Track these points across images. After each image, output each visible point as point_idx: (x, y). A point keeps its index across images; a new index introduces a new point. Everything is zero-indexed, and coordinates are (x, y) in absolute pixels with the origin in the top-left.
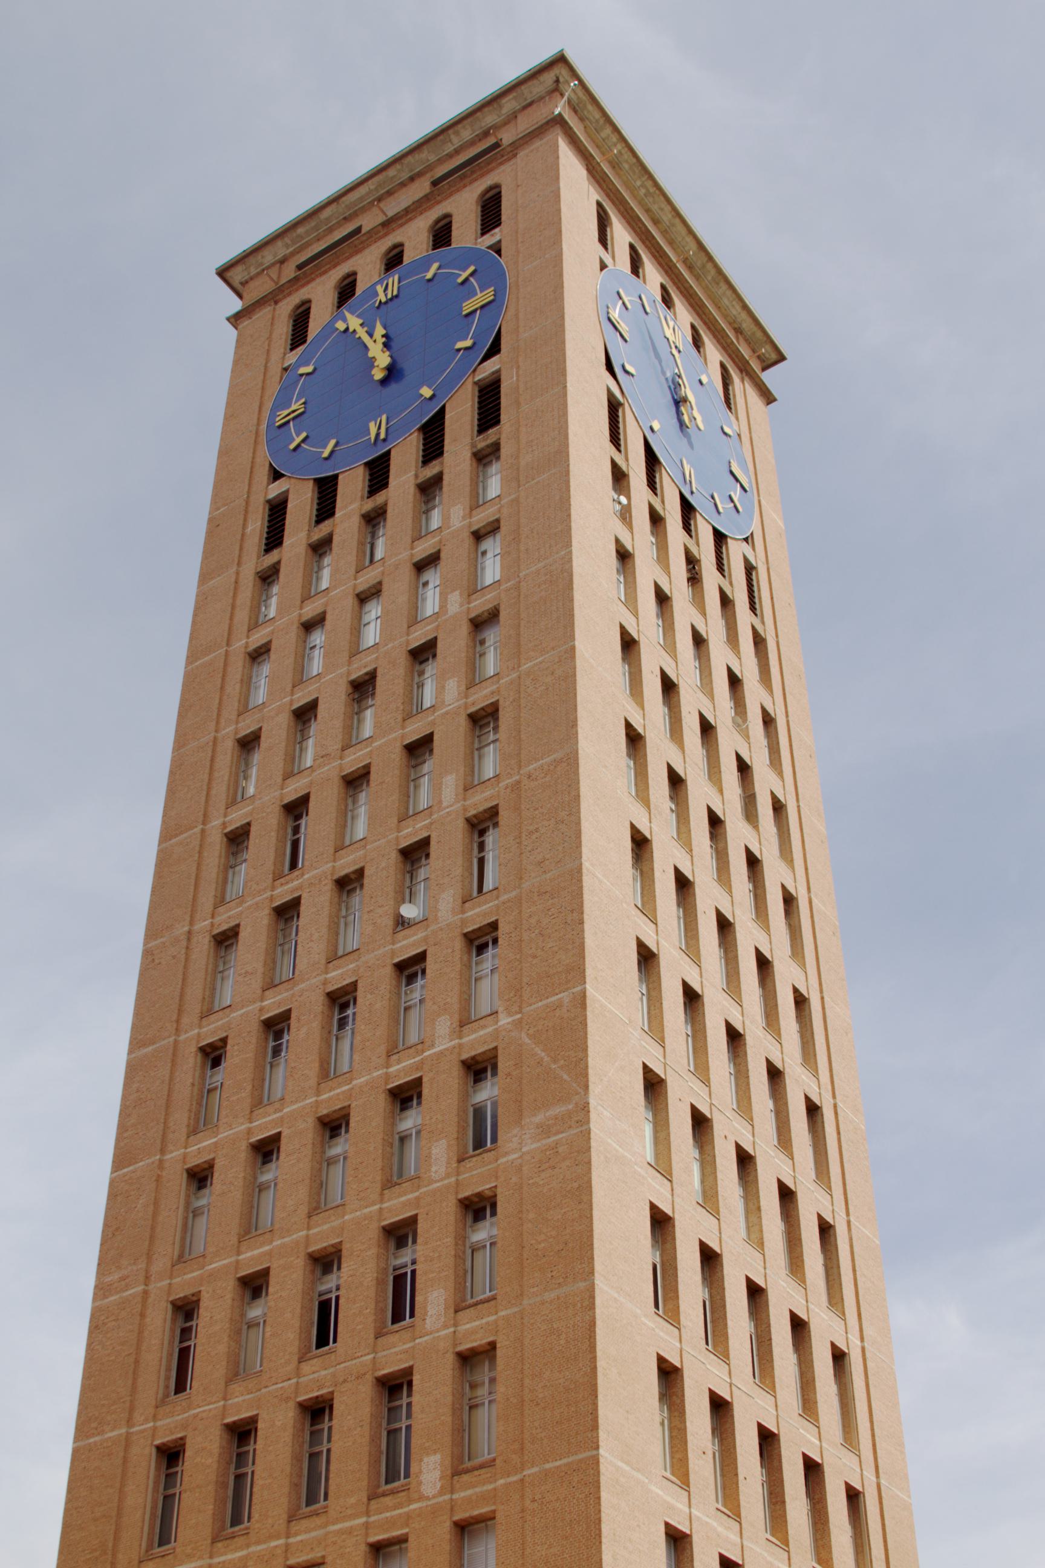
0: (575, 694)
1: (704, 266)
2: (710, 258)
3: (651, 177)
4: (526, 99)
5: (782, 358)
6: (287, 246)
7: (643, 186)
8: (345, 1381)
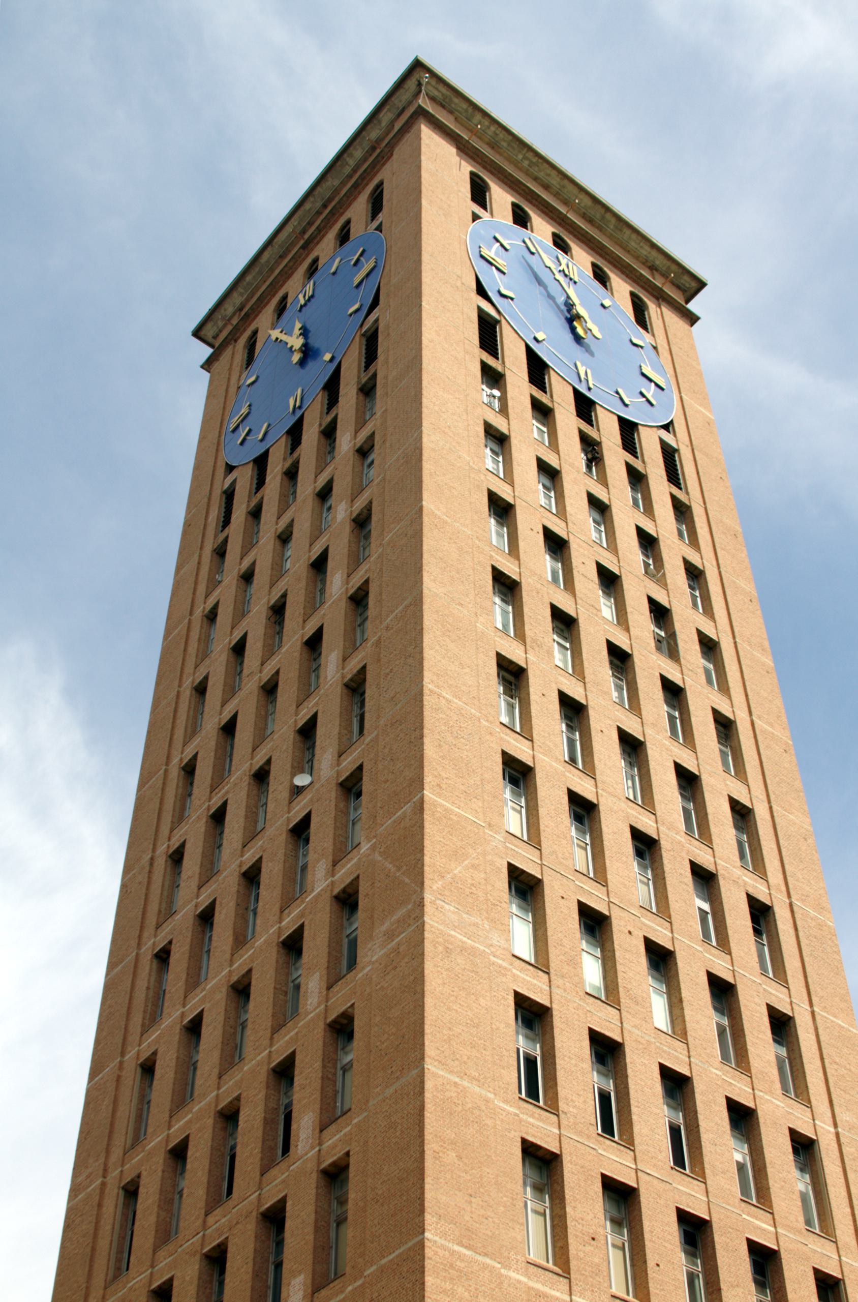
0: (422, 545)
1: (603, 217)
2: (607, 209)
3: (530, 149)
4: (398, 108)
5: (702, 285)
6: (242, 295)
7: (525, 158)
8: (237, 1223)
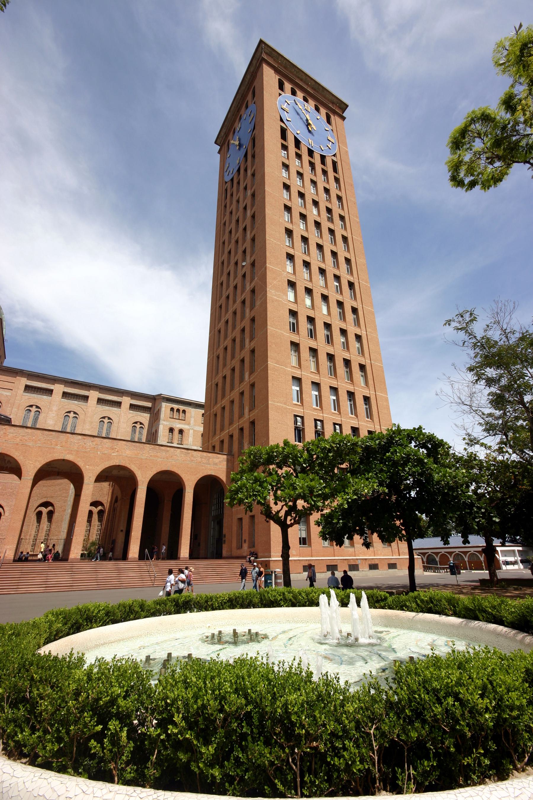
2: (319, 85)
7: (295, 70)
